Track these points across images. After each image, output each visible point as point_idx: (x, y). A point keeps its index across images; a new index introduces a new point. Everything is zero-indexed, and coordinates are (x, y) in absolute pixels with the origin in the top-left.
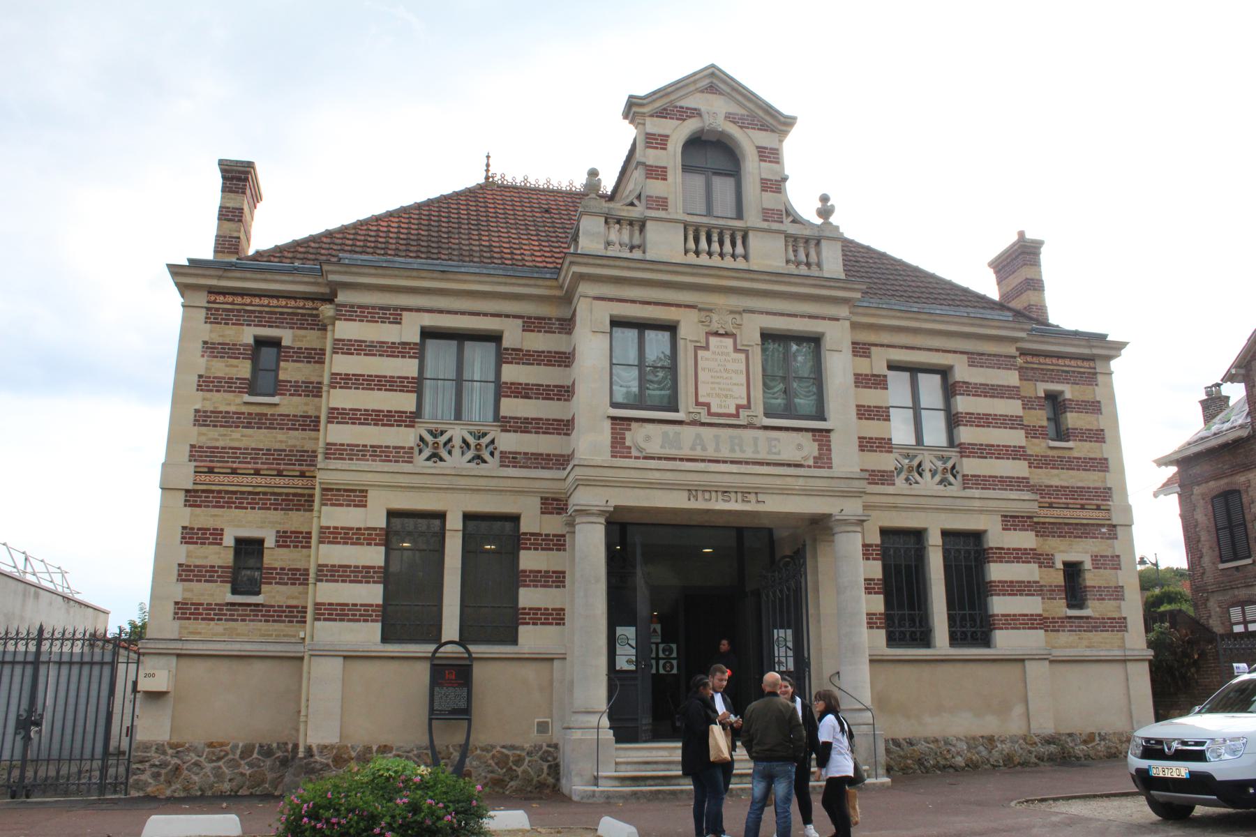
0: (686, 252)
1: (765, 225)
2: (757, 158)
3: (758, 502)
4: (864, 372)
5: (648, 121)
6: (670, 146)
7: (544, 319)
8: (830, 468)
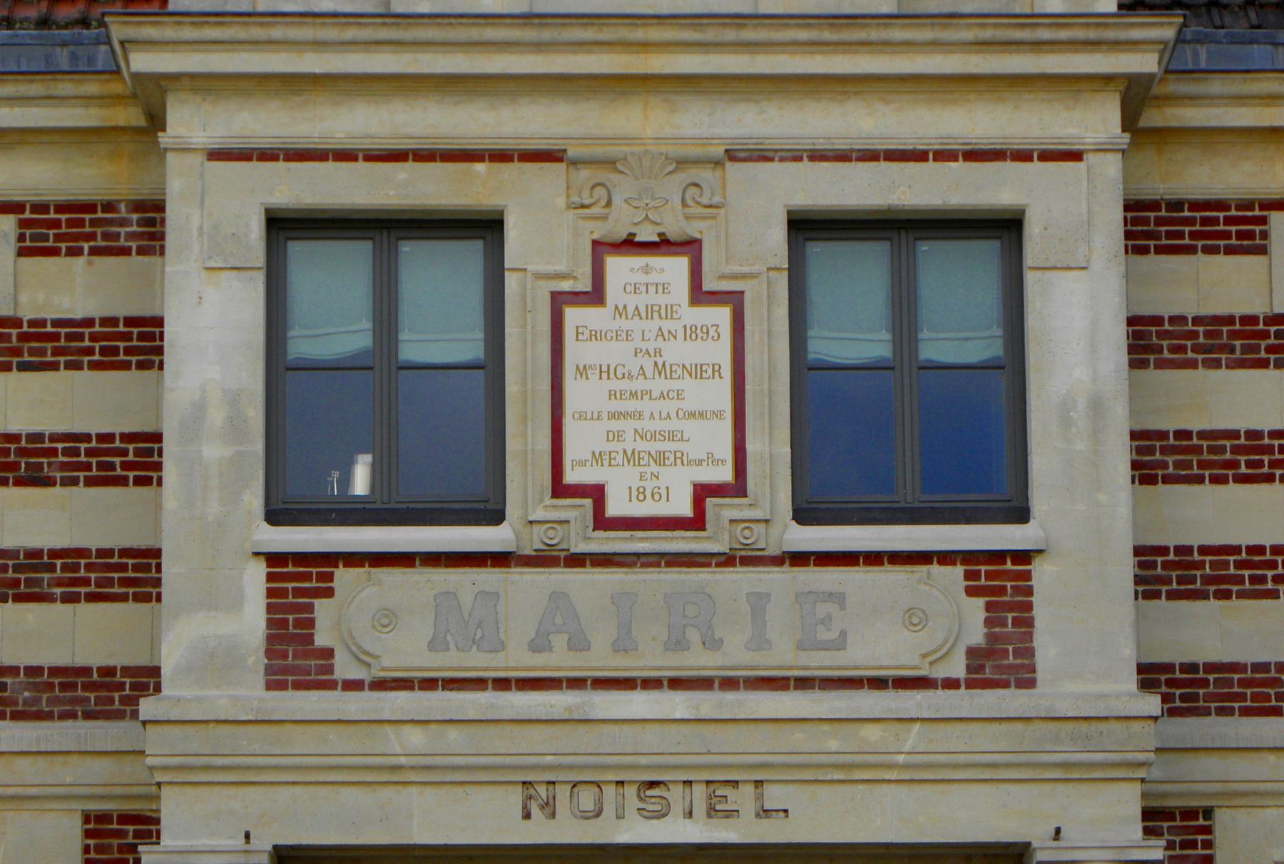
3: (765, 813)
4: (1239, 310)
7: (89, 207)
8: (1030, 683)
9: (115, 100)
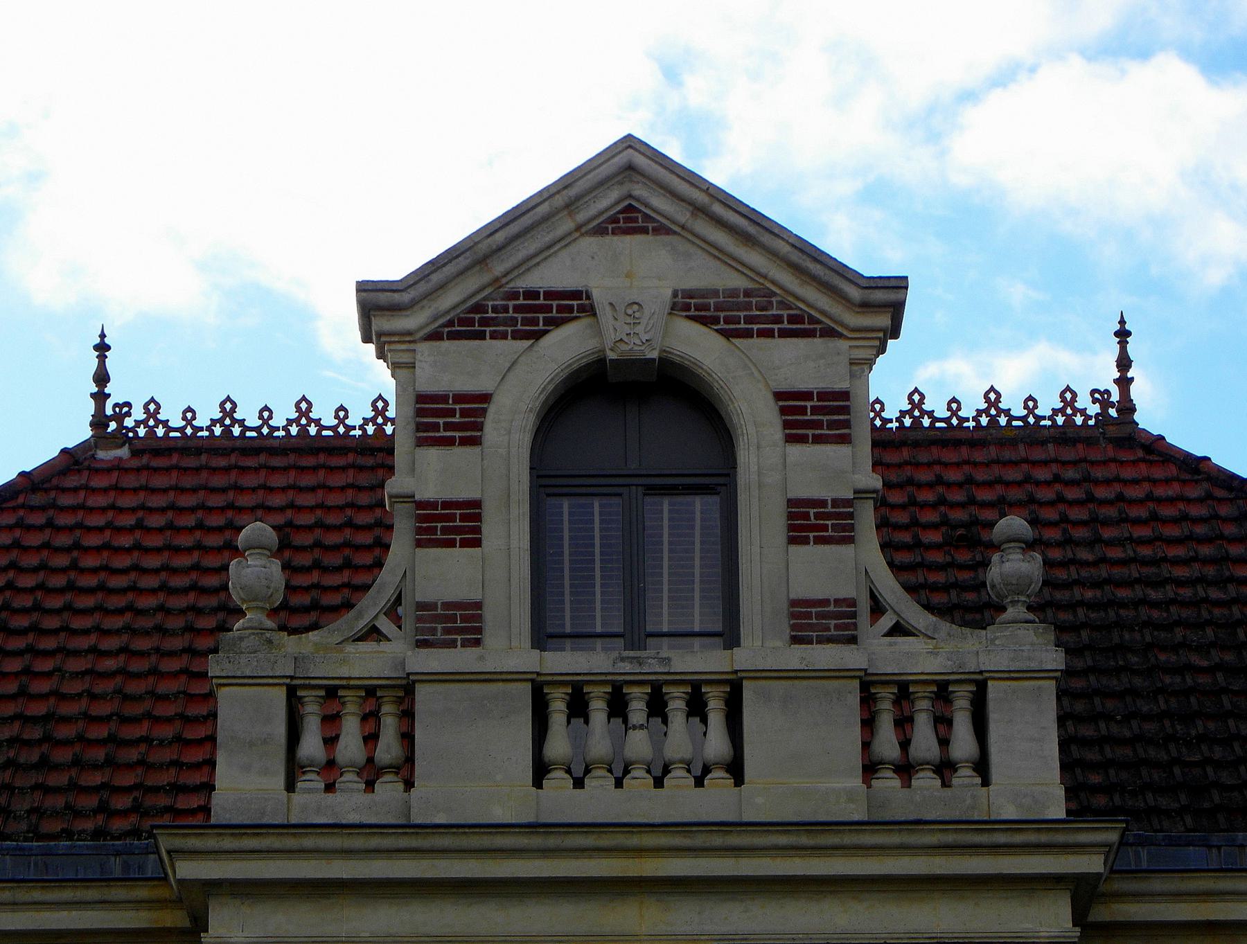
0: (541, 771)
1: (796, 657)
2: (775, 432)
5: (424, 348)
6: (491, 432)
9: (160, 904)
